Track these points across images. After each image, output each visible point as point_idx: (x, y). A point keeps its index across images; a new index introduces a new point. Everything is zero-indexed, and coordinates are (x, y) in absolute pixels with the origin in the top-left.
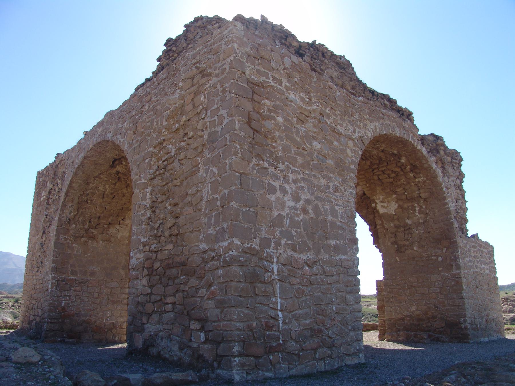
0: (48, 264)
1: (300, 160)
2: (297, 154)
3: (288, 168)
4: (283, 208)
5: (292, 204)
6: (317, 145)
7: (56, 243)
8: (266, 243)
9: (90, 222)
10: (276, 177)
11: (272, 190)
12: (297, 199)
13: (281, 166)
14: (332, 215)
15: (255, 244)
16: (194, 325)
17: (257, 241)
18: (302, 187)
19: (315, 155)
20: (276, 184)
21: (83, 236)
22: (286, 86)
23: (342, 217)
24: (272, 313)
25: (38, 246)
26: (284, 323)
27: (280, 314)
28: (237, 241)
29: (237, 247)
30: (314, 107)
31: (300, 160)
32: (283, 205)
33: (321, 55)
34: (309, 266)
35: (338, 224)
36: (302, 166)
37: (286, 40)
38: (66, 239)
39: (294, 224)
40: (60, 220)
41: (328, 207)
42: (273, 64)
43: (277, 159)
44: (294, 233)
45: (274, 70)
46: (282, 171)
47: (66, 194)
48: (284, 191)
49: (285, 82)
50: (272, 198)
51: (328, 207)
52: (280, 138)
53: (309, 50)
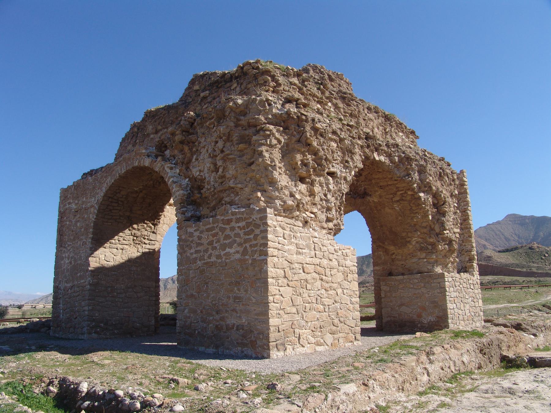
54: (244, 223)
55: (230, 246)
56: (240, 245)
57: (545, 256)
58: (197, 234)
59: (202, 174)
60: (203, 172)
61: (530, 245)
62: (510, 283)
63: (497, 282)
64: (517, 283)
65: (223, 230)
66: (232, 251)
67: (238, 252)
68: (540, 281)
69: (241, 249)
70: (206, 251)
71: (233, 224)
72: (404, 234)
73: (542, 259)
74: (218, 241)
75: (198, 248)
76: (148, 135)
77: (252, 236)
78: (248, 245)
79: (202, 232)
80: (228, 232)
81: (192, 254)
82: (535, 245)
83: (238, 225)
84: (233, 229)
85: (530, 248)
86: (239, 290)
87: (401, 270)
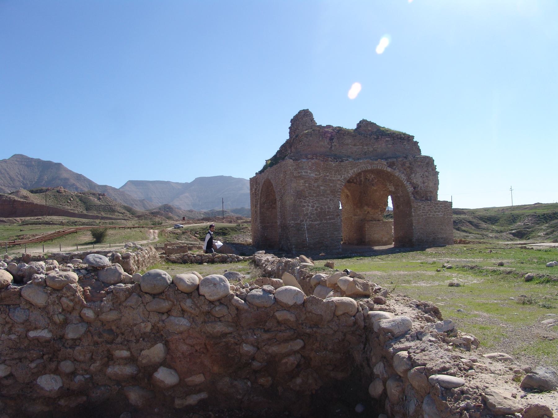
0: (258, 220)
1: (315, 195)
2: (313, 193)
3: (310, 198)
4: (308, 211)
5: (312, 209)
6: (322, 188)
7: (260, 212)
8: (303, 221)
9: (272, 202)
10: (305, 202)
11: (304, 206)
12: (313, 207)
13: (307, 199)
14: (328, 209)
15: (299, 222)
16: (288, 242)
17: (299, 221)
18: (316, 203)
19: (321, 191)
20: (306, 204)
21: (270, 208)
22: (309, 173)
23: (333, 209)
24: (304, 238)
25: (254, 212)
26: (308, 240)
27: (307, 238)
28: (293, 222)
29: (293, 223)
30: (322, 175)
31: (315, 195)
32: (308, 210)
33: (342, 135)
34: (318, 225)
35: (331, 211)
36: (316, 196)
37: (325, 135)
38: (263, 210)
39: (312, 214)
40: (260, 204)
41: (326, 207)
42: (304, 167)
43: (306, 197)
44: (312, 216)
45: (304, 169)
46: (308, 200)
47: (261, 194)
48: (308, 206)
49: (309, 171)
50: (304, 209)
51: (326, 207)
52: (307, 190)
53: (336, 135)
54: (444, 205)
55: (439, 212)
56: (442, 212)
57: (70, 200)
58: (423, 206)
59: (417, 183)
60: (418, 181)
61: (58, 189)
62: (88, 224)
63: (76, 222)
64: (94, 224)
65: (435, 206)
66: (439, 214)
67: (442, 214)
68: (113, 223)
69: (443, 214)
70: (428, 212)
71: (439, 205)
72: (379, 204)
73: (68, 202)
74: (433, 210)
75: (423, 211)
76: (348, 144)
77: (447, 210)
78: (445, 212)
79: (425, 206)
80: (437, 207)
81: (421, 213)
82: (62, 190)
83: (441, 205)
84: (439, 206)
85: (58, 192)
86: (442, 226)
87: (370, 219)
